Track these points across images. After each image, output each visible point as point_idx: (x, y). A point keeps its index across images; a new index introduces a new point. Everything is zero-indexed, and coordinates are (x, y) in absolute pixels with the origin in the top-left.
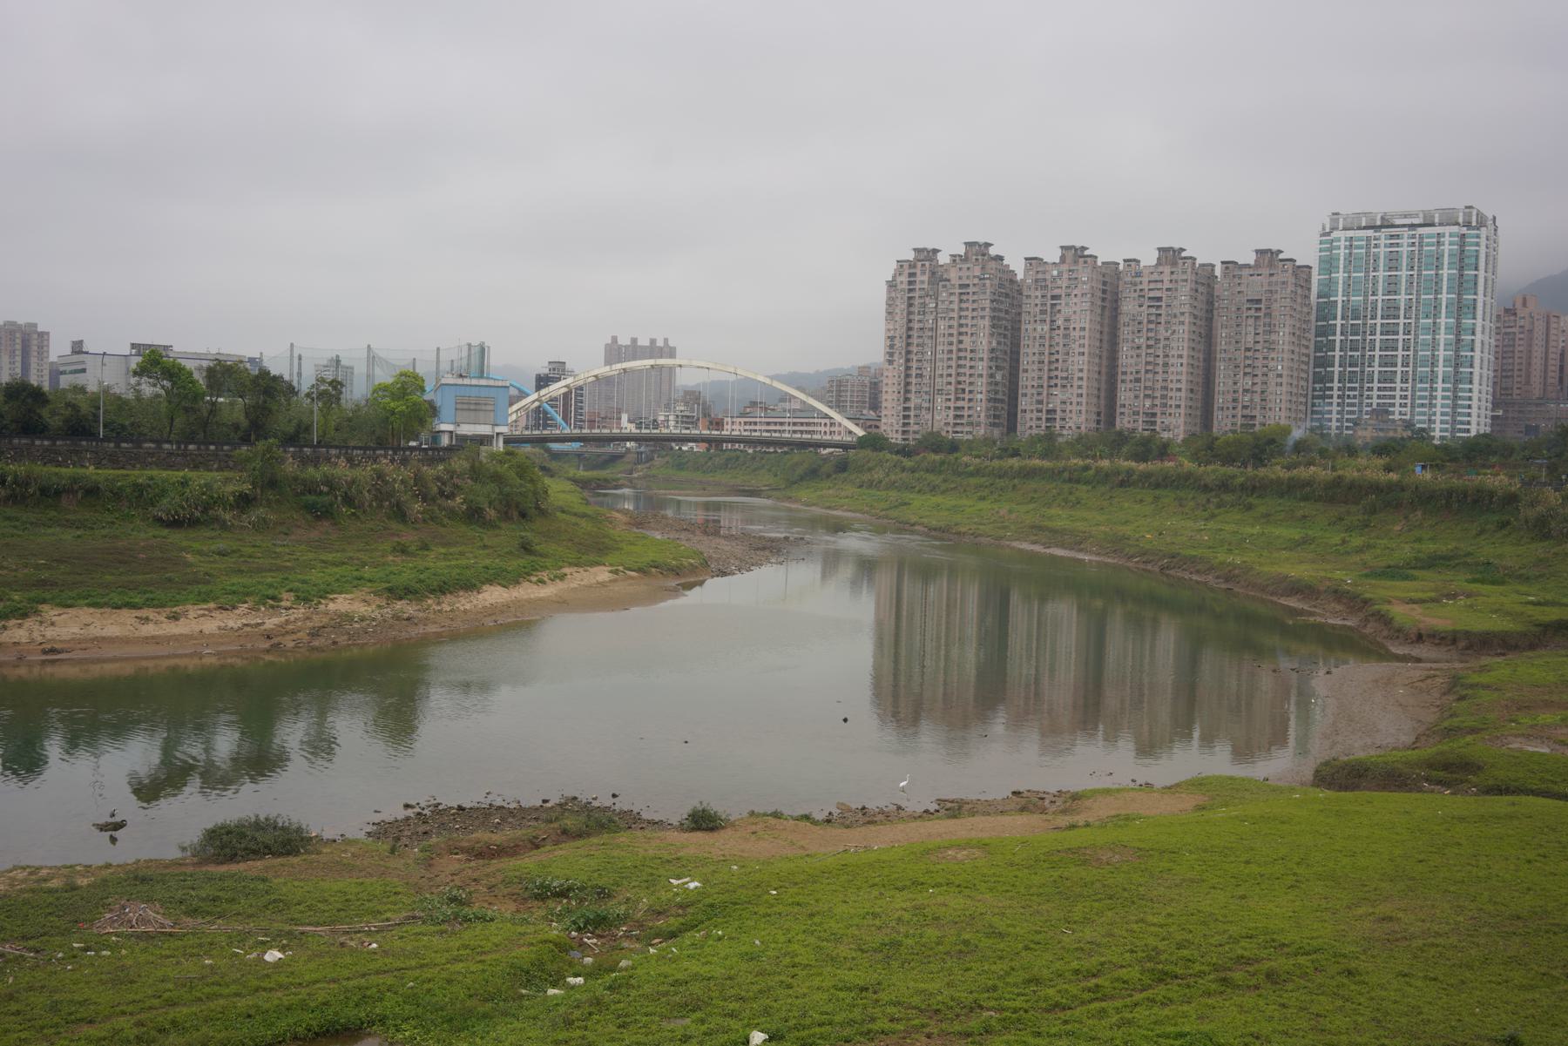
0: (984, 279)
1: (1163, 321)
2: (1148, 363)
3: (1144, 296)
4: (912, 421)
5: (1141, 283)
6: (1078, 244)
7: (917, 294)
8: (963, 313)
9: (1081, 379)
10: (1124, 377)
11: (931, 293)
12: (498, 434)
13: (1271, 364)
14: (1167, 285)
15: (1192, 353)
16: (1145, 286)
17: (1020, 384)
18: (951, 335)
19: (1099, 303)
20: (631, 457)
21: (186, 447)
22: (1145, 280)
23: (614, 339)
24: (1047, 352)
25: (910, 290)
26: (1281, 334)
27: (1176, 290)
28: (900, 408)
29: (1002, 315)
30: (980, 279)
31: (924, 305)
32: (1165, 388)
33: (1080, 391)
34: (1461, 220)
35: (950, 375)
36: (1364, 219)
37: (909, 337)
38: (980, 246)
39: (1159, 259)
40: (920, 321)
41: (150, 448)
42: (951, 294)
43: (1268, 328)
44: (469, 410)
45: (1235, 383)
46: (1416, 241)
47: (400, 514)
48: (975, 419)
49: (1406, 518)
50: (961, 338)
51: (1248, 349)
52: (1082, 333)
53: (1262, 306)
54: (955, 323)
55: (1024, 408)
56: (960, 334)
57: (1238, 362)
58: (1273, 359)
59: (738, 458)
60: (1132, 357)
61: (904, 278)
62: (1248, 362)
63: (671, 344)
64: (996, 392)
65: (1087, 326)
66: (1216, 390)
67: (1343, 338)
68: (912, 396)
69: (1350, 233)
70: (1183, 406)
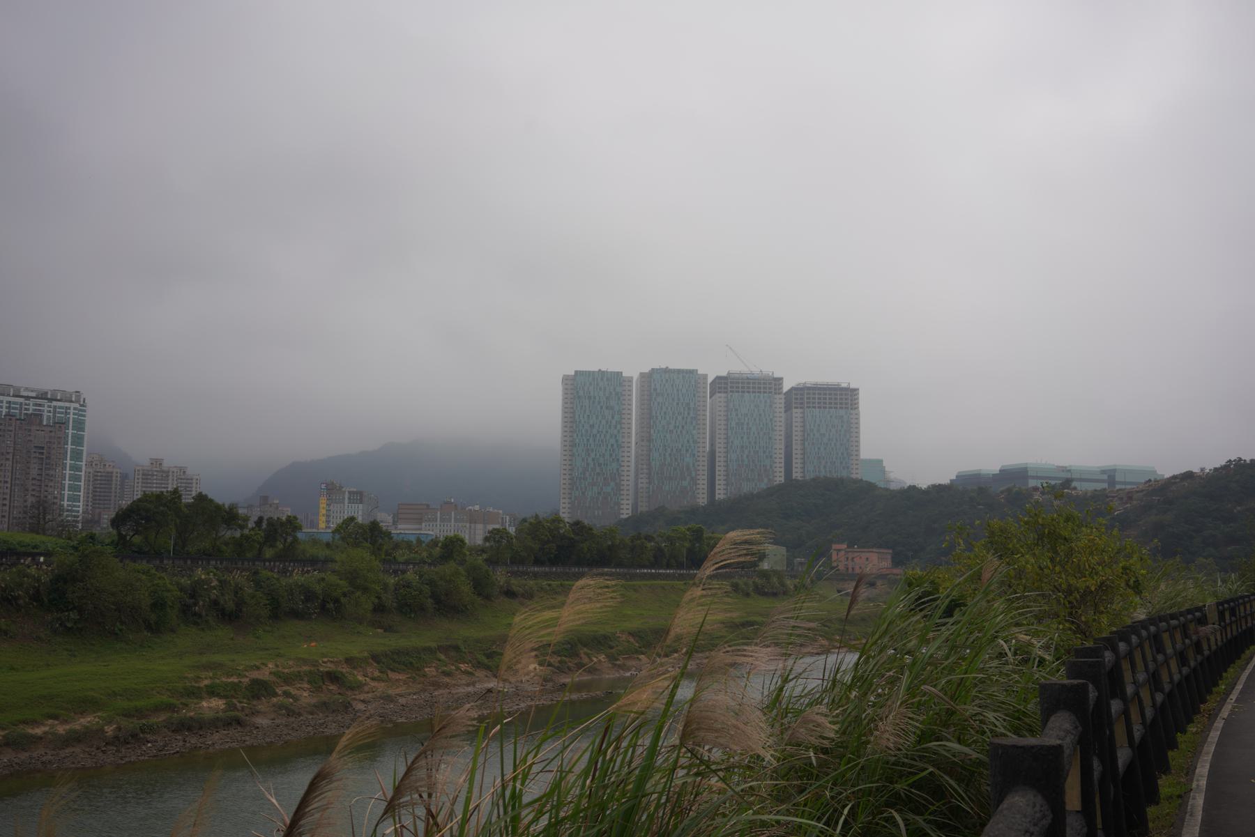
13: (50, 490)
26: (57, 471)
34: (73, 399)
36: (12, 390)
46: (51, 409)
51: (33, 479)
53: (45, 451)
58: (51, 487)
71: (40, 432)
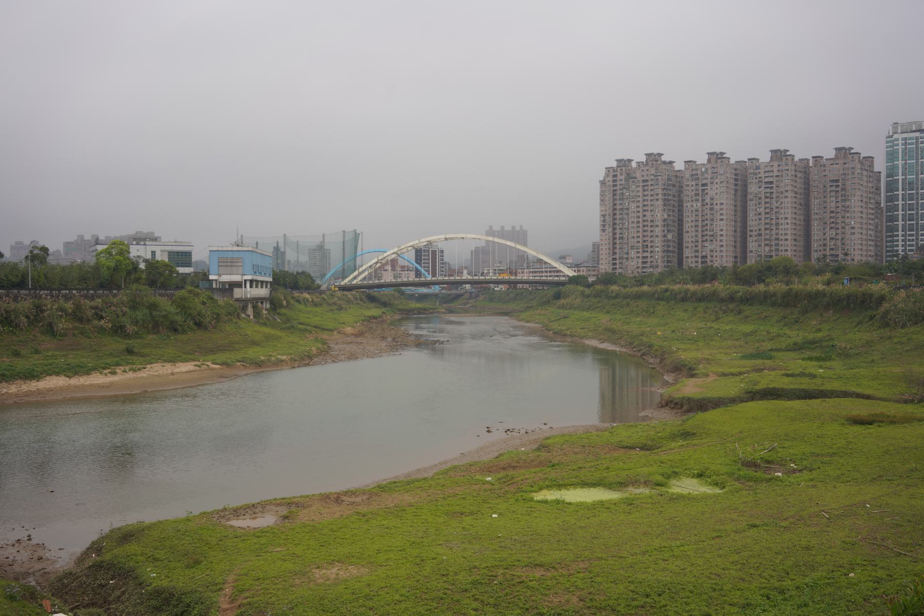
0: (657, 176)
1: (774, 196)
2: (766, 224)
3: (761, 181)
4: (618, 267)
5: (759, 173)
6: (718, 151)
7: (618, 188)
8: (645, 198)
9: (722, 235)
10: (751, 233)
11: (626, 187)
12: (245, 281)
14: (776, 173)
15: (795, 216)
16: (762, 175)
17: (684, 241)
18: (639, 212)
19: (733, 187)
20: (467, 295)
22: (762, 171)
23: (491, 227)
24: (700, 220)
25: (615, 185)
26: (853, 201)
27: (782, 176)
28: (610, 259)
29: (671, 198)
30: (655, 176)
31: (622, 194)
32: (777, 239)
33: (721, 243)
35: (639, 237)
37: (615, 214)
38: (655, 155)
39: (771, 157)
40: (621, 204)
42: (638, 186)
43: (844, 198)
44: (227, 266)
45: (825, 234)
47: (50, 330)
48: (655, 263)
49: (821, 315)
50: (645, 213)
51: (832, 212)
52: (722, 207)
53: (840, 184)
54: (640, 204)
55: (687, 255)
56: (644, 211)
57: (826, 220)
58: (848, 217)
59: (522, 293)
60: (756, 220)
61: (610, 178)
62: (832, 220)
63: (524, 228)
64: (669, 246)
65: (724, 202)
66: (812, 239)
67: (904, 202)
68: (617, 251)
69: (905, 135)
70: (789, 250)
71: (834, 166)
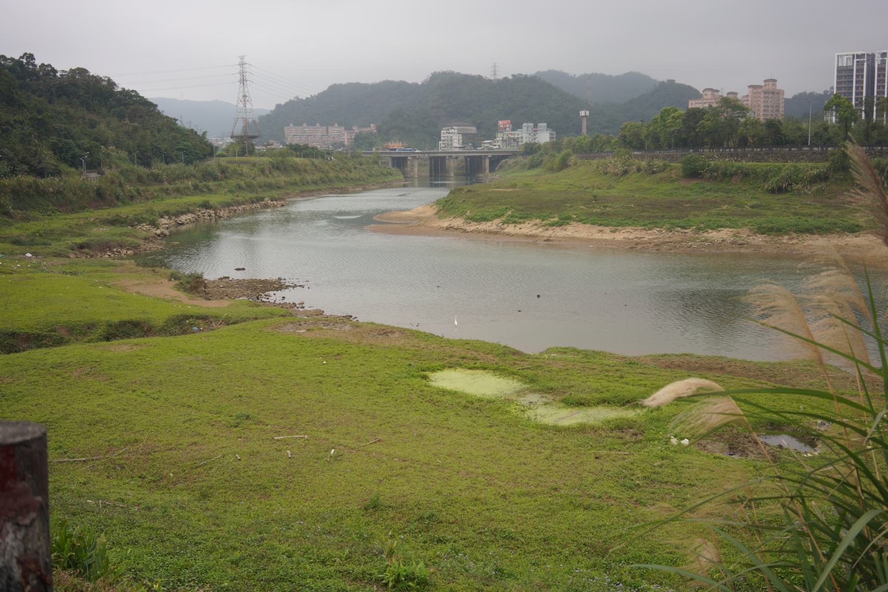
21: (827, 149)
41: (806, 150)
